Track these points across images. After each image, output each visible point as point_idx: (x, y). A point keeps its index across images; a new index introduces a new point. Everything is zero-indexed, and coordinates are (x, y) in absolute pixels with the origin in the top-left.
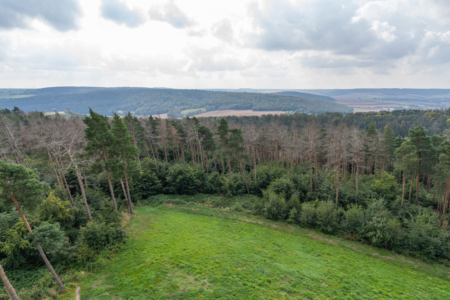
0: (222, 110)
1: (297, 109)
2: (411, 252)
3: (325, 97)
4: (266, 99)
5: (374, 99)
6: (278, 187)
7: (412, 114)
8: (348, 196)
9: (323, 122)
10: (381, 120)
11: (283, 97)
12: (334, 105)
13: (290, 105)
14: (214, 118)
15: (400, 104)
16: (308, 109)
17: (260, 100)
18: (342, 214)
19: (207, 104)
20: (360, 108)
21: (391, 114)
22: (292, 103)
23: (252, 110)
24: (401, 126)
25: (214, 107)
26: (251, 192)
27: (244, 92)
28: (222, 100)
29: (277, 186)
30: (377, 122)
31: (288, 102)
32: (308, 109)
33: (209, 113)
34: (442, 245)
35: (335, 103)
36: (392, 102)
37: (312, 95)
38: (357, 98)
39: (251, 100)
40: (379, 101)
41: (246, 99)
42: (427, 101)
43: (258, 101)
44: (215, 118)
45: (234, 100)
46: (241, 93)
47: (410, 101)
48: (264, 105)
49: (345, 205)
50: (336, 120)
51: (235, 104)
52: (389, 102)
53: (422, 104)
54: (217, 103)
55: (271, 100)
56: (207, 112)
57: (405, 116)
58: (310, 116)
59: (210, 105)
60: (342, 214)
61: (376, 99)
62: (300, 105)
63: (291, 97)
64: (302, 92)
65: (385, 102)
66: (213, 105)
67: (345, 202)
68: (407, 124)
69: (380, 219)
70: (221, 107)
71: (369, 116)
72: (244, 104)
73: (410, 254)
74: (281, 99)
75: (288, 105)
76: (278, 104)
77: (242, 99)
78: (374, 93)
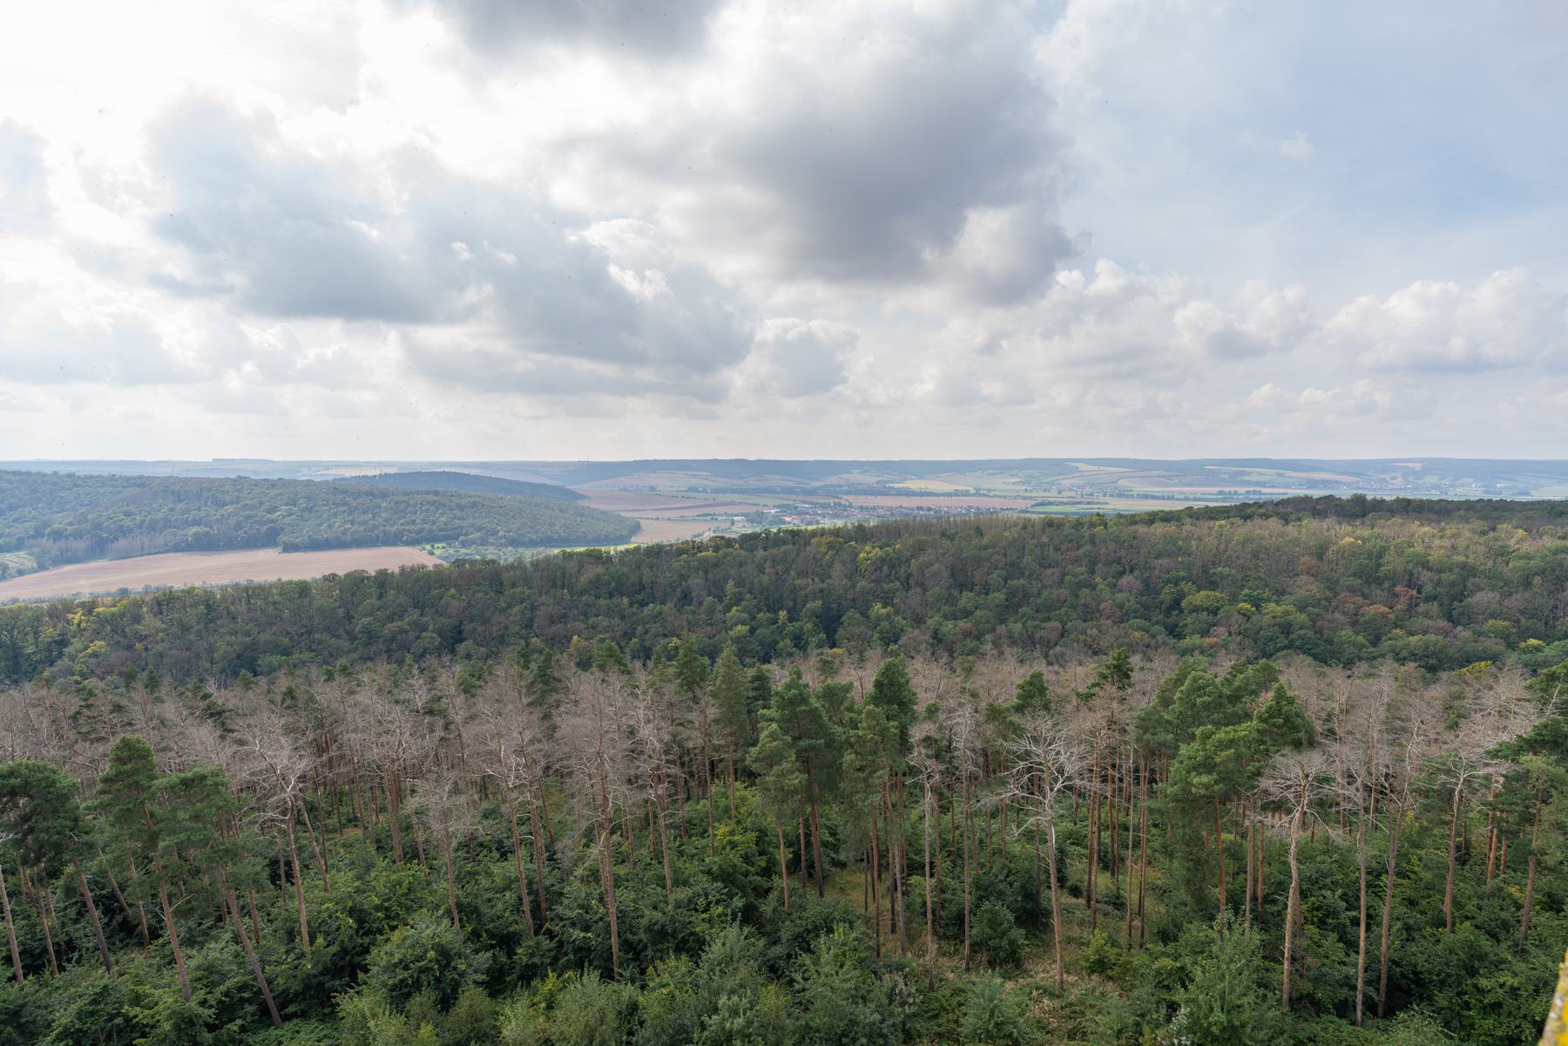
0: (126, 555)
1: (460, 535)
3: (553, 489)
4: (337, 505)
5: (690, 489)
6: (406, 968)
7: (785, 542)
8: (644, 922)
9: (554, 586)
10: (716, 565)
11: (405, 494)
13: (434, 523)
14: (83, 604)
15: (755, 505)
16: (501, 534)
17: (310, 510)
18: (634, 1008)
19: (38, 534)
20: (657, 519)
21: (737, 546)
22: (442, 514)
23: (280, 549)
24: (765, 579)
25: (80, 545)
26: (291, 1009)
27: (234, 476)
28: (127, 514)
29: (401, 961)
30: (706, 572)
31: (427, 511)
32: (501, 534)
33: (53, 572)
34: (883, 1020)
37: (510, 482)
39: (272, 510)
40: (703, 496)
41: (246, 507)
42: (813, 492)
43: (303, 510)
44: (89, 607)
45: (188, 511)
46: (223, 482)
47: (778, 493)
48: (330, 526)
49: (641, 951)
50: (591, 576)
51: (195, 529)
52: (729, 497)
53: (805, 502)
54: (98, 526)
55: (356, 508)
56: (42, 567)
58: (511, 567)
59: (58, 535)
60: (634, 1008)
62: (470, 520)
63: (436, 493)
64: (473, 472)
65: (721, 498)
66: (77, 535)
67: (641, 941)
68: (777, 574)
69: (735, 998)
70: (122, 543)
71: (684, 556)
72: (239, 526)
74: (397, 503)
75: (425, 521)
76: (386, 521)
77: (230, 508)
78: (689, 473)
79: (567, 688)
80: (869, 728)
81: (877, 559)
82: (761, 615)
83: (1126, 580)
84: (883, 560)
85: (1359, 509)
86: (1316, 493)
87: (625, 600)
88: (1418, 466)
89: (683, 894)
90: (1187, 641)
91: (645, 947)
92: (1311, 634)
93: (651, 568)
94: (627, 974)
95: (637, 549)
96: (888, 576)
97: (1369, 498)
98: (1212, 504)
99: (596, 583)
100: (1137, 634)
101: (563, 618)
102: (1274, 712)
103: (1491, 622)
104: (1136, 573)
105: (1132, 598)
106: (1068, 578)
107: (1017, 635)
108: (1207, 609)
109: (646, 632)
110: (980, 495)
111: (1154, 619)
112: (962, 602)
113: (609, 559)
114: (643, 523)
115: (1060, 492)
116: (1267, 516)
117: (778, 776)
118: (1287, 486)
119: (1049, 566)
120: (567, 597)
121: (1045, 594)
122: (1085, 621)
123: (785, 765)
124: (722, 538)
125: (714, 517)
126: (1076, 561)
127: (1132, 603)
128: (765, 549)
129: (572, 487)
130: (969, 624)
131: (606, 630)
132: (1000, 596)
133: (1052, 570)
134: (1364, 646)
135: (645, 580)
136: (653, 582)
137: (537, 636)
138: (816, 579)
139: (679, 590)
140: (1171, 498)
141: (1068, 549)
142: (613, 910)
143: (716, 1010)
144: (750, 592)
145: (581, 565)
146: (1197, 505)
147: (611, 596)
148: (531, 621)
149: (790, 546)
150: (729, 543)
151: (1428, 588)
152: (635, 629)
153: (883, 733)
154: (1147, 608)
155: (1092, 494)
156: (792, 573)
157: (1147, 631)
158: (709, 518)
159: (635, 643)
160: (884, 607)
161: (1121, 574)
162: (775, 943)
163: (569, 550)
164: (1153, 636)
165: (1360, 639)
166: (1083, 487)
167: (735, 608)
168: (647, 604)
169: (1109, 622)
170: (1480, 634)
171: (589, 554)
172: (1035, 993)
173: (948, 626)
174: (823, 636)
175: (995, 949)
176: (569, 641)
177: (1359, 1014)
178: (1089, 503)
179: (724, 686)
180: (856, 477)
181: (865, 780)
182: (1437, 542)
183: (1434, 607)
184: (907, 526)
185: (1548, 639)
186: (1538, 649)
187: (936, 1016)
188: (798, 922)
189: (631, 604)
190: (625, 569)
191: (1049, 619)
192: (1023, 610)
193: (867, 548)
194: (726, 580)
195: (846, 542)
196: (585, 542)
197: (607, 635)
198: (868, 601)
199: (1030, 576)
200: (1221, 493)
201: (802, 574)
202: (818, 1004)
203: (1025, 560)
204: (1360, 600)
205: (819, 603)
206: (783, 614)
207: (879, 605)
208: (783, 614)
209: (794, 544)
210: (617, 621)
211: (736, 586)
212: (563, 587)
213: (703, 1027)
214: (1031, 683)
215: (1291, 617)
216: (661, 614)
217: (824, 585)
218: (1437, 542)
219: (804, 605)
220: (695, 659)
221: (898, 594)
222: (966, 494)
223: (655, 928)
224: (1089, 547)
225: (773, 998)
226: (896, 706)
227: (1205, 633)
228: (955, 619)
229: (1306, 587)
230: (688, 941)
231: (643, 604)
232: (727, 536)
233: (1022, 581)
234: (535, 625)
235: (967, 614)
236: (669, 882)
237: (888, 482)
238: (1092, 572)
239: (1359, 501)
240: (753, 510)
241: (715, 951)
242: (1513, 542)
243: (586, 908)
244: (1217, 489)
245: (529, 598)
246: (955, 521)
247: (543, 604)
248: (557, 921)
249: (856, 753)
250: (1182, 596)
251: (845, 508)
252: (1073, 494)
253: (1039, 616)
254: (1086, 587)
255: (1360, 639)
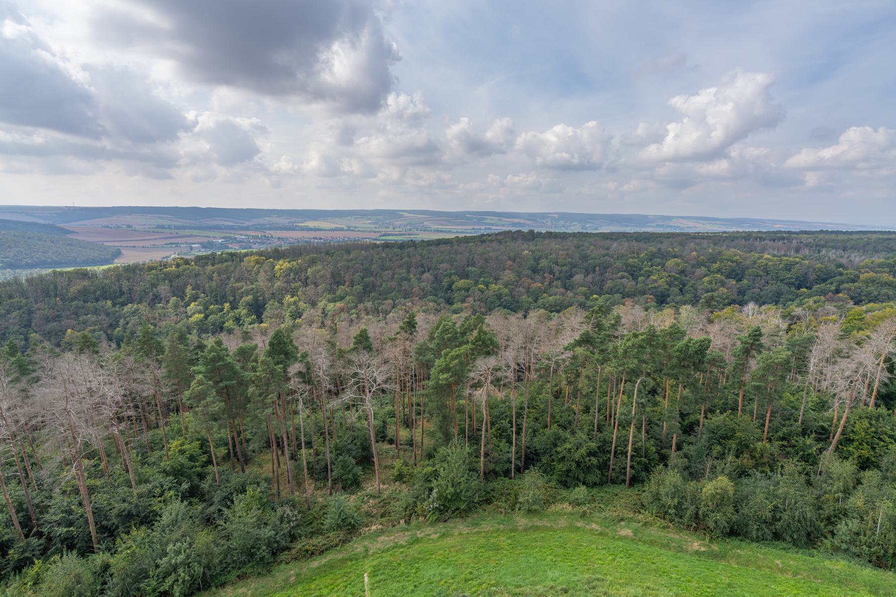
2: (239, 572)
3: (44, 226)
5: (159, 227)
7: (226, 261)
8: (115, 511)
9: (48, 295)
10: (178, 276)
12: (71, 245)
21: (193, 263)
24: (214, 284)
30: (171, 281)
34: (277, 533)
35: (72, 240)
36: (193, 232)
38: (124, 227)
40: (168, 231)
42: (247, 228)
47: (222, 229)
49: (114, 530)
50: (79, 287)
52: (188, 232)
53: (242, 235)
57: (216, 266)
60: (106, 567)
61: (162, 227)
65: (182, 232)
68: (221, 280)
69: (179, 544)
71: (154, 271)
73: (238, 577)
79: (43, 367)
80: (263, 370)
81: (287, 269)
82: (212, 306)
83: (426, 276)
84: (291, 269)
85: (532, 236)
86: (514, 229)
87: (109, 303)
88: (557, 216)
89: (144, 488)
90: (455, 306)
91: (117, 527)
92: (510, 298)
93: (128, 280)
94: (104, 546)
95: (117, 268)
96: (294, 279)
97: (535, 231)
98: (468, 235)
99: (84, 294)
100: (431, 304)
101: (57, 319)
102: (477, 339)
103: (580, 288)
104: (431, 271)
105: (429, 285)
106: (396, 276)
107: (369, 309)
108: (464, 289)
109: (127, 323)
110: (351, 230)
111: (440, 295)
112: (339, 292)
113: (95, 275)
114: (123, 251)
115: (394, 229)
116: (491, 241)
117: (205, 406)
118: (503, 225)
119: (386, 270)
120: (60, 303)
121: (384, 285)
122: (405, 298)
123: (208, 399)
124: (182, 259)
125: (177, 245)
126: (400, 266)
127: (428, 288)
128: (213, 265)
129: (62, 225)
130: (343, 304)
131: (94, 324)
132: (359, 288)
133: (387, 272)
134: (531, 303)
135: (124, 289)
136: (130, 289)
137: (36, 332)
138: (248, 283)
139: (151, 294)
140: (450, 232)
141: (396, 260)
142: (89, 509)
143: (166, 554)
144: (204, 293)
145: (70, 281)
146: (461, 235)
147: (97, 300)
148: (30, 322)
149: (229, 263)
150: (187, 262)
151: (557, 274)
152: (118, 321)
153: (272, 373)
154: (436, 290)
155: (411, 230)
156: (232, 279)
157: (435, 302)
158: (174, 246)
159: (119, 331)
160: (292, 297)
161: (423, 272)
162: (211, 505)
163: (58, 270)
164: (439, 305)
165: (530, 299)
166: (406, 226)
167: (193, 303)
168: (127, 304)
169: (417, 298)
170: (576, 294)
171: (77, 273)
172: (365, 498)
173: (331, 306)
174: (254, 317)
175: (346, 480)
176: (64, 334)
177: (513, 474)
178: (409, 235)
179: (170, 354)
180: (275, 219)
181: (263, 401)
182: (561, 252)
183: (559, 283)
184: (305, 249)
185: (600, 294)
186: (596, 299)
187: (311, 523)
188: (225, 489)
189: (114, 305)
190: (107, 281)
191: (386, 299)
192: (372, 295)
193: (281, 262)
194: (185, 286)
195: (267, 259)
196: (74, 263)
197: (96, 327)
198: (282, 294)
199: (376, 275)
200: (473, 229)
201: (238, 280)
202: (235, 534)
203: (373, 267)
204: (530, 281)
205: (250, 297)
206: (227, 306)
207: (289, 296)
208: (227, 306)
209: (233, 261)
210: (103, 317)
211: (193, 289)
212: (56, 296)
213: (157, 566)
214: (360, 336)
215: (501, 291)
216: (138, 310)
217: (254, 286)
218: (561, 252)
219: (241, 297)
220: (152, 338)
221: (301, 289)
222: (342, 230)
223: (124, 513)
224: (406, 259)
225: (203, 538)
226: (283, 356)
227: (463, 301)
228: (335, 302)
229: (508, 276)
230: (149, 517)
231: (124, 304)
232: (185, 257)
233: (371, 279)
234: (33, 324)
235: (342, 298)
236: (133, 483)
237: (295, 222)
238: (408, 272)
239: (531, 232)
240: (205, 240)
241: (166, 519)
242: (589, 252)
243: (70, 512)
244: (471, 227)
245: (26, 305)
246: (334, 245)
247: (39, 309)
248: (46, 524)
249: (257, 386)
250: (453, 283)
251: (268, 238)
252: (401, 229)
253: (381, 297)
254: (405, 280)
255: (530, 299)
